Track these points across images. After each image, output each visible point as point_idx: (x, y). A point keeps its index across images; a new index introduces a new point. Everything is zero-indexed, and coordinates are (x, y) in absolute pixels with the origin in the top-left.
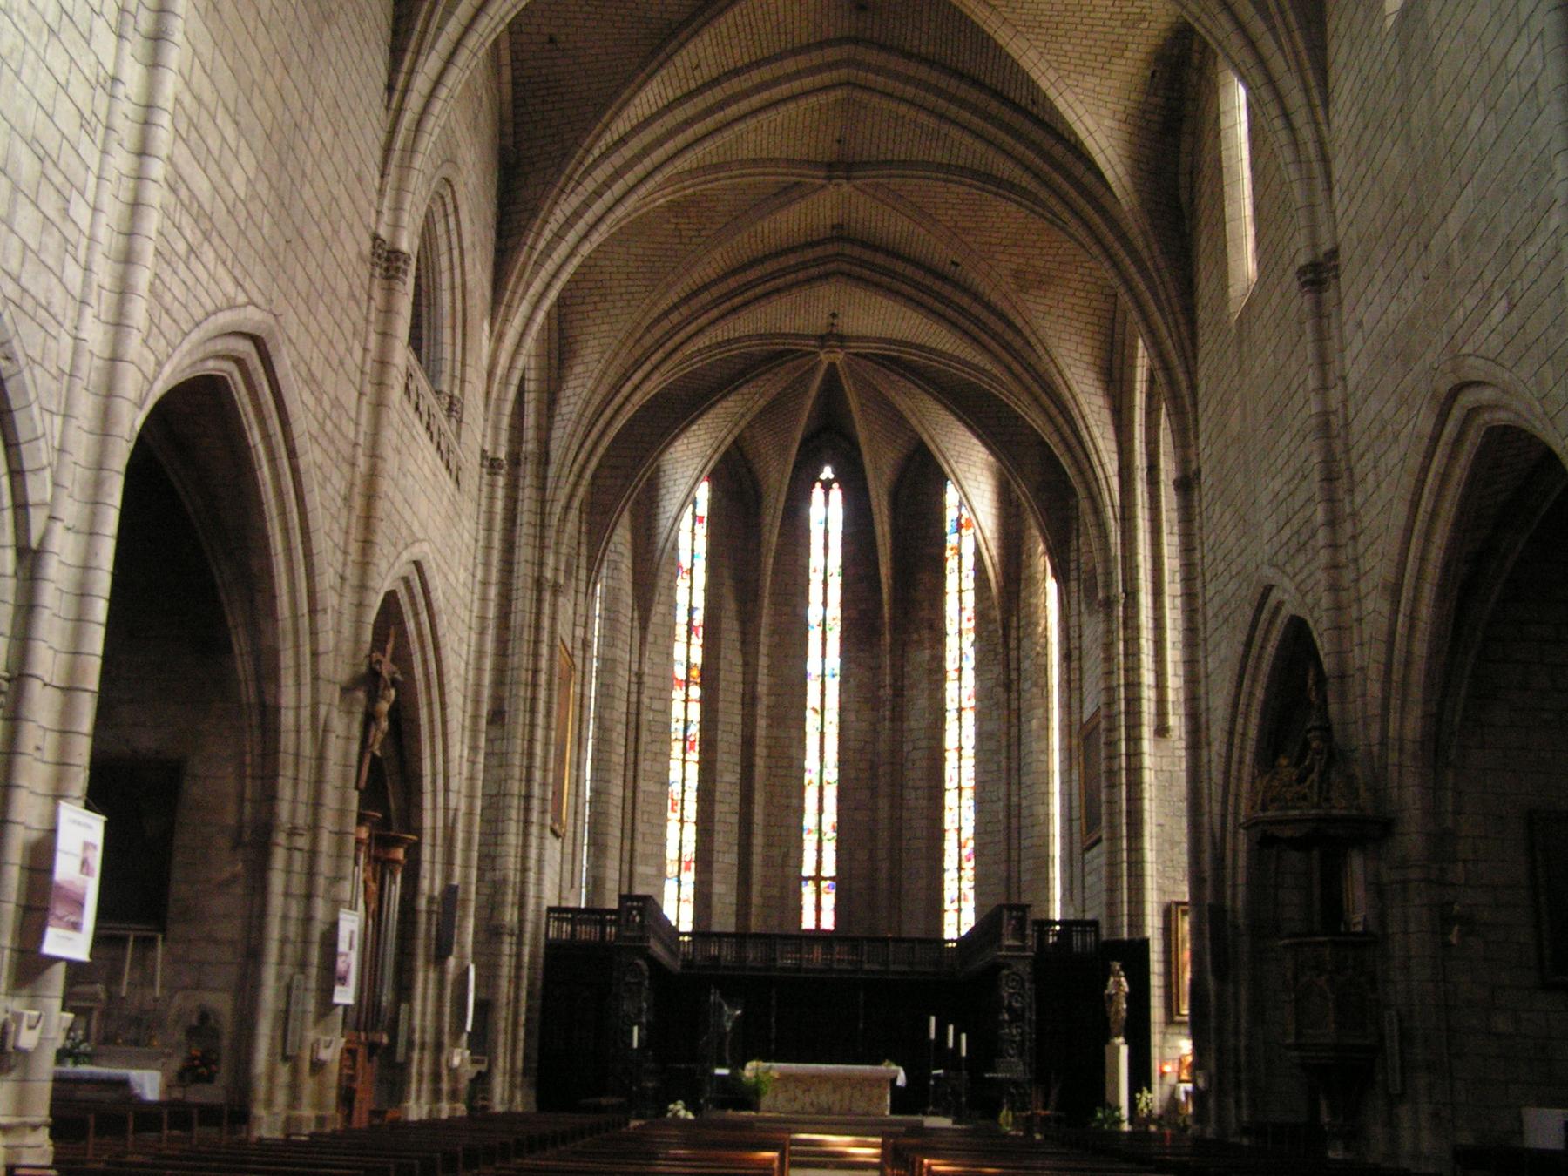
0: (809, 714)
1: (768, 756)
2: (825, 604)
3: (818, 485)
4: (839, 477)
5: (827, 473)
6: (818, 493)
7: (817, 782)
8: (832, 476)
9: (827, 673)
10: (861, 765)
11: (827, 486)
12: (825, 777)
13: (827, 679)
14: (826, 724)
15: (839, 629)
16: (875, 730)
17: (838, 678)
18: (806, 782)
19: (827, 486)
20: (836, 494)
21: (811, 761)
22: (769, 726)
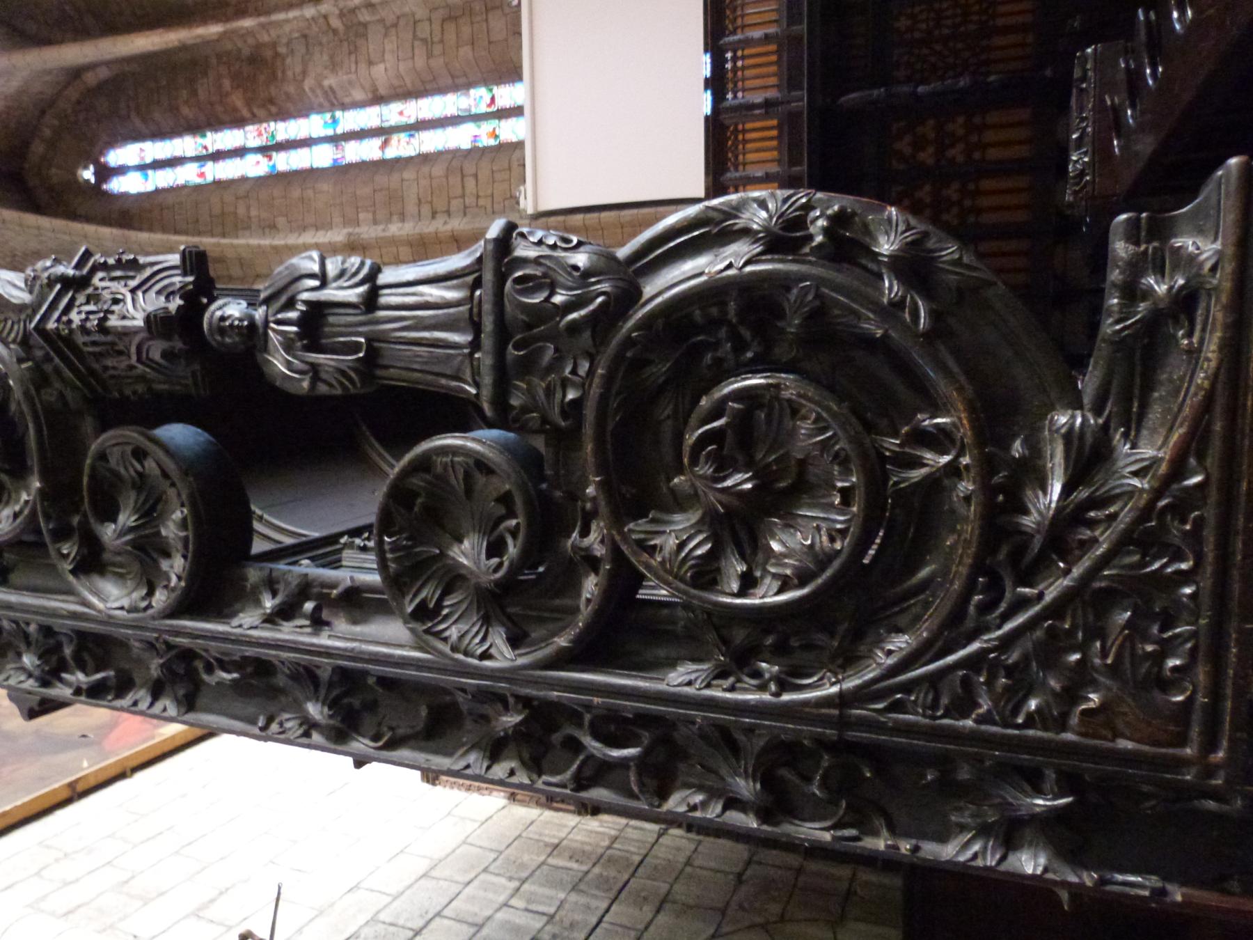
0: (391, 153)
1: (448, 213)
2: (240, 152)
3: (104, 187)
4: (92, 155)
5: (88, 174)
6: (117, 185)
7: (488, 126)
8: (92, 168)
9: (330, 132)
10: (451, 36)
11: (105, 173)
12: (483, 109)
13: (339, 131)
14: (403, 120)
15: (272, 124)
16: (395, 25)
17: (338, 114)
18: (492, 142)
19: (105, 173)
20: (115, 157)
21: (460, 138)
22: (403, 217)
